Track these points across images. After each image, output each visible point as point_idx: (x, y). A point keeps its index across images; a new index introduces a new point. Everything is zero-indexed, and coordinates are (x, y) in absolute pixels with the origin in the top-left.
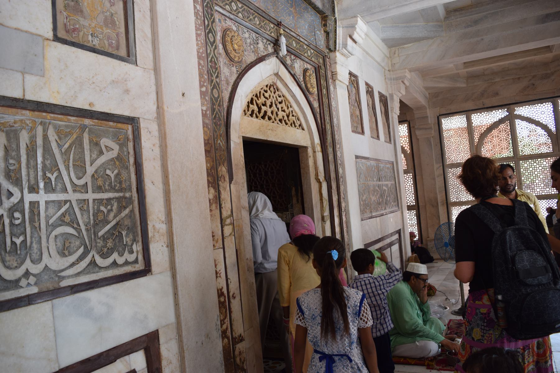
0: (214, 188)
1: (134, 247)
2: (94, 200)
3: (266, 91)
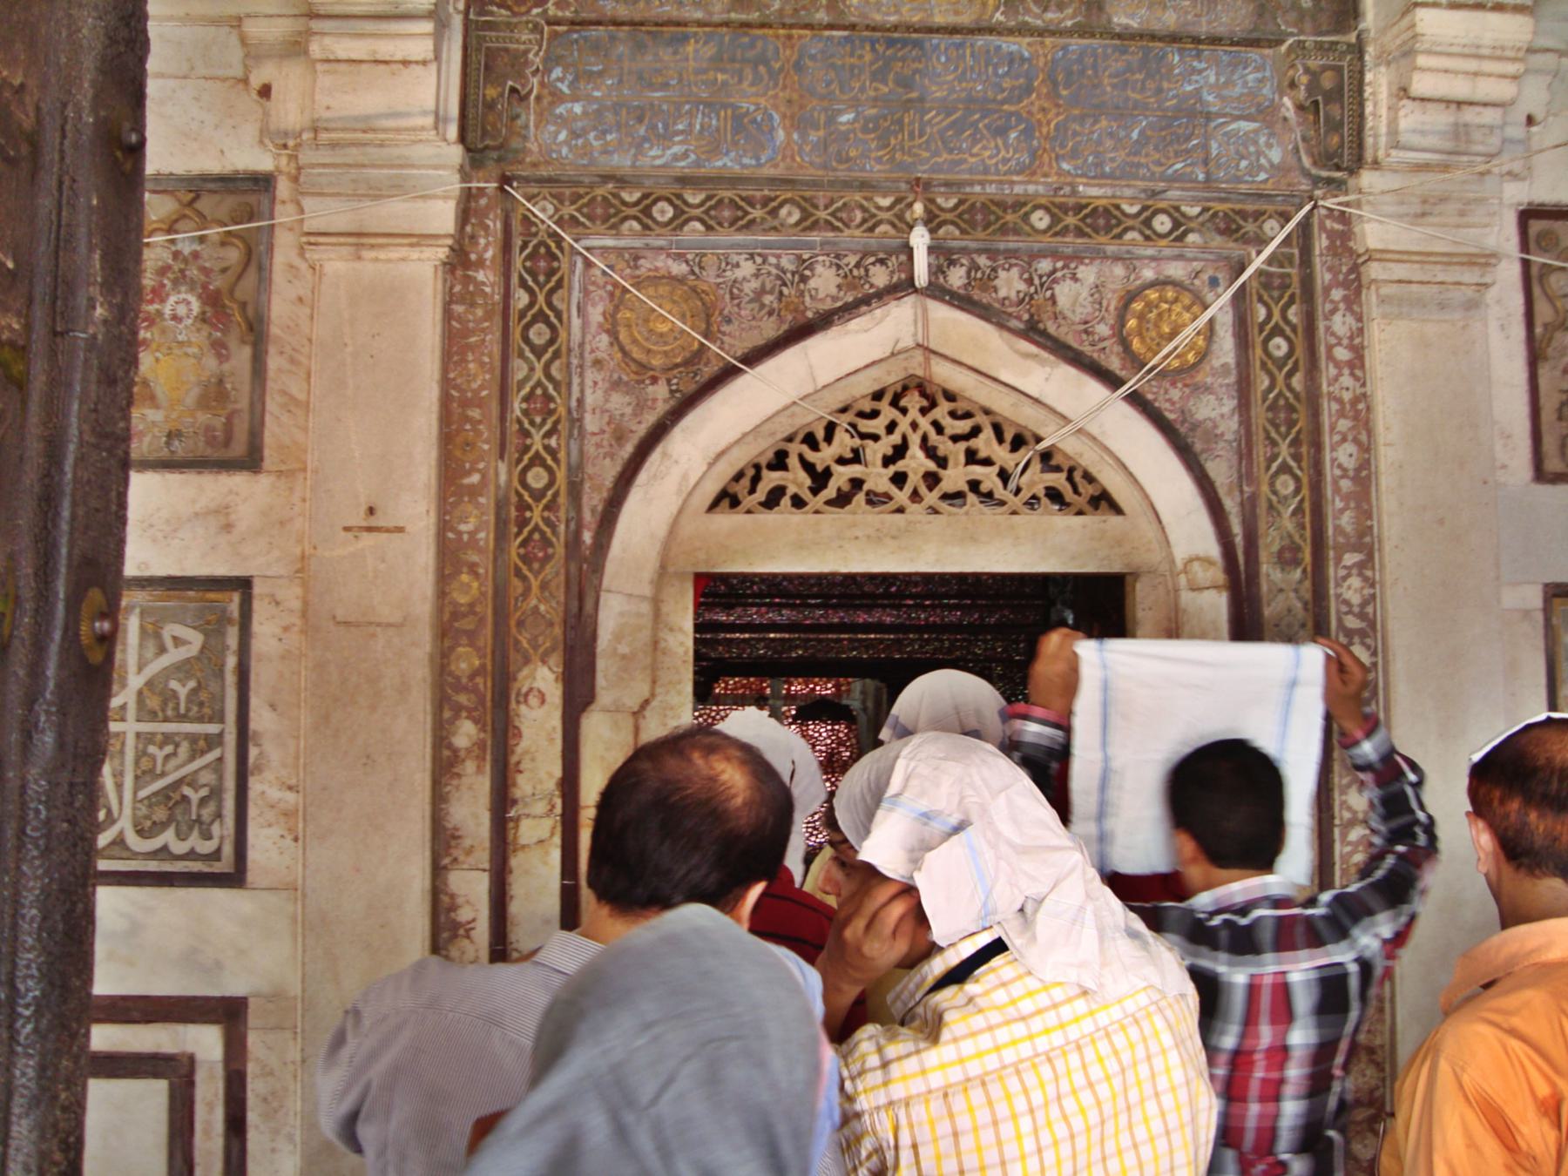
0: (476, 722)
1: (216, 829)
2: (138, 735)
3: (874, 414)
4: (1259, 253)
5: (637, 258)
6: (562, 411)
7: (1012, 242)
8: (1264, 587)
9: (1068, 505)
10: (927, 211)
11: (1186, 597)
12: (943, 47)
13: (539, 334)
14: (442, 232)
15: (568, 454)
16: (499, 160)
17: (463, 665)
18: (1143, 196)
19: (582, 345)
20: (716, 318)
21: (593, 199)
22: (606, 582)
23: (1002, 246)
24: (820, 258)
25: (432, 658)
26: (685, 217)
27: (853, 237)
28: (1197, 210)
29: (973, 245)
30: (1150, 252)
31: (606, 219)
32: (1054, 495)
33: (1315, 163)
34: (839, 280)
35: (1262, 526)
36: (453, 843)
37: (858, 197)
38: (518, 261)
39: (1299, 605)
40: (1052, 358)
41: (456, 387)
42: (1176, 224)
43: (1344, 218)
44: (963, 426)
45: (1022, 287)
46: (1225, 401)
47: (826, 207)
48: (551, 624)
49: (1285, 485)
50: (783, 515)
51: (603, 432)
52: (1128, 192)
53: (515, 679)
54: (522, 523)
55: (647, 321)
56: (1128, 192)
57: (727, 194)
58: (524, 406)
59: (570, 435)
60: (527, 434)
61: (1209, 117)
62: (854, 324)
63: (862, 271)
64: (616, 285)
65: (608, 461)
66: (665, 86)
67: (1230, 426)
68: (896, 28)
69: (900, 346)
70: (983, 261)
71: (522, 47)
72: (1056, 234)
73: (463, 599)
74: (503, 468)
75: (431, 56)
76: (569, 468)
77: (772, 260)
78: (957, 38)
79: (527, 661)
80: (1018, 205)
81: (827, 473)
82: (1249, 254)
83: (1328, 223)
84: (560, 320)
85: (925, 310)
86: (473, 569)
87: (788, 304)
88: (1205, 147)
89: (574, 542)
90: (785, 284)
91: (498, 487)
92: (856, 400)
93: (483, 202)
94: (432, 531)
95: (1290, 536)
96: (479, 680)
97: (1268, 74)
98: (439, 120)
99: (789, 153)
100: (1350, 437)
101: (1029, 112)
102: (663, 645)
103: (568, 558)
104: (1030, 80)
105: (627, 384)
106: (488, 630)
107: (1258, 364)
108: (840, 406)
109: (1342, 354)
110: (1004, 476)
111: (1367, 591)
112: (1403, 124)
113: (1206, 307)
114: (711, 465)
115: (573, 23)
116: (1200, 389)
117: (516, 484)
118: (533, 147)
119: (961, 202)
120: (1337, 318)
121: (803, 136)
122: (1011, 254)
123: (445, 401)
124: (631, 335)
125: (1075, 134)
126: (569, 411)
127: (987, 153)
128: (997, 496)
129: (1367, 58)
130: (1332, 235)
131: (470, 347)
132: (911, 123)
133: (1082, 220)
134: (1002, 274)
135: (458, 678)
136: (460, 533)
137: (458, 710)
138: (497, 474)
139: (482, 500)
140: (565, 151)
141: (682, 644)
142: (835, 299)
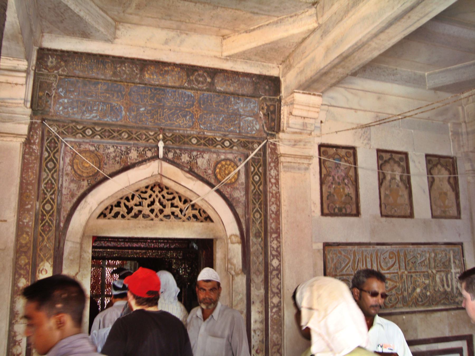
0: (26, 279)
3: (146, 192)
4: (252, 153)
5: (80, 145)
6: (56, 188)
7: (186, 147)
8: (251, 243)
9: (198, 219)
10: (163, 136)
11: (230, 245)
12: (170, 92)
13: (51, 165)
14: (23, 133)
15: (57, 200)
16: (42, 114)
17: (23, 262)
18: (222, 136)
19: (63, 169)
20: (102, 163)
21: (69, 127)
22: (67, 238)
23: (183, 147)
24: (133, 148)
25: (13, 259)
26: (95, 134)
27: (142, 143)
28: (236, 140)
29: (175, 147)
30: (223, 151)
31: (72, 133)
32: (195, 216)
33: (268, 129)
34: (138, 154)
35: (251, 227)
36: (16, 316)
37: (144, 132)
38: (45, 143)
39: (260, 248)
40: (196, 179)
41: (25, 179)
42: (231, 144)
43: (275, 145)
44: (171, 197)
45: (188, 159)
46: (242, 192)
47: (135, 134)
48: (50, 250)
49: (257, 216)
50: (119, 221)
51: (68, 194)
52: (218, 135)
53: (38, 266)
54: (42, 220)
55: (82, 163)
56: (218, 135)
57: (107, 128)
58: (45, 186)
59: (58, 195)
60: (45, 194)
61: (240, 116)
62: (142, 167)
63: (144, 152)
64: (74, 152)
65: (69, 203)
66: (92, 96)
67: (243, 199)
68: (158, 85)
69: (154, 174)
70: (178, 151)
71: (51, 82)
72: (198, 145)
73: (24, 242)
74: (38, 204)
75: (25, 83)
76: (57, 204)
77: (119, 148)
78: (174, 89)
79: (42, 260)
80: (188, 136)
81: (132, 208)
82: (250, 153)
83: (271, 146)
84: (57, 161)
85: (161, 164)
86: (27, 233)
87: (123, 160)
88: (239, 124)
89: (58, 226)
90: (122, 155)
91: (36, 209)
92: (141, 188)
93: (36, 125)
94: (15, 222)
95: (258, 229)
96: (28, 266)
97: (256, 105)
98: (25, 101)
99: (125, 118)
100: (275, 203)
101: (193, 112)
102: (82, 256)
103: (56, 231)
104: (193, 102)
105: (75, 181)
106: (31, 252)
107: (251, 182)
108: (136, 189)
109: (273, 181)
110: (181, 211)
111: (278, 245)
112: (290, 122)
113: (238, 167)
114: (99, 205)
115: (66, 76)
116: (235, 189)
117: (41, 208)
118: (53, 111)
119: (173, 135)
120: (272, 171)
121: (130, 113)
122: (186, 150)
123: (21, 183)
124: (78, 167)
125: (205, 118)
126: (58, 188)
127: (180, 122)
128: (179, 216)
129: (282, 103)
130: (271, 149)
131: (30, 168)
132: (160, 112)
133: (206, 142)
134: (183, 155)
135: (21, 266)
136: (23, 223)
137: (20, 275)
138: (36, 205)
139: (31, 213)
140: (61, 113)
141: (88, 256)
142: (136, 160)
